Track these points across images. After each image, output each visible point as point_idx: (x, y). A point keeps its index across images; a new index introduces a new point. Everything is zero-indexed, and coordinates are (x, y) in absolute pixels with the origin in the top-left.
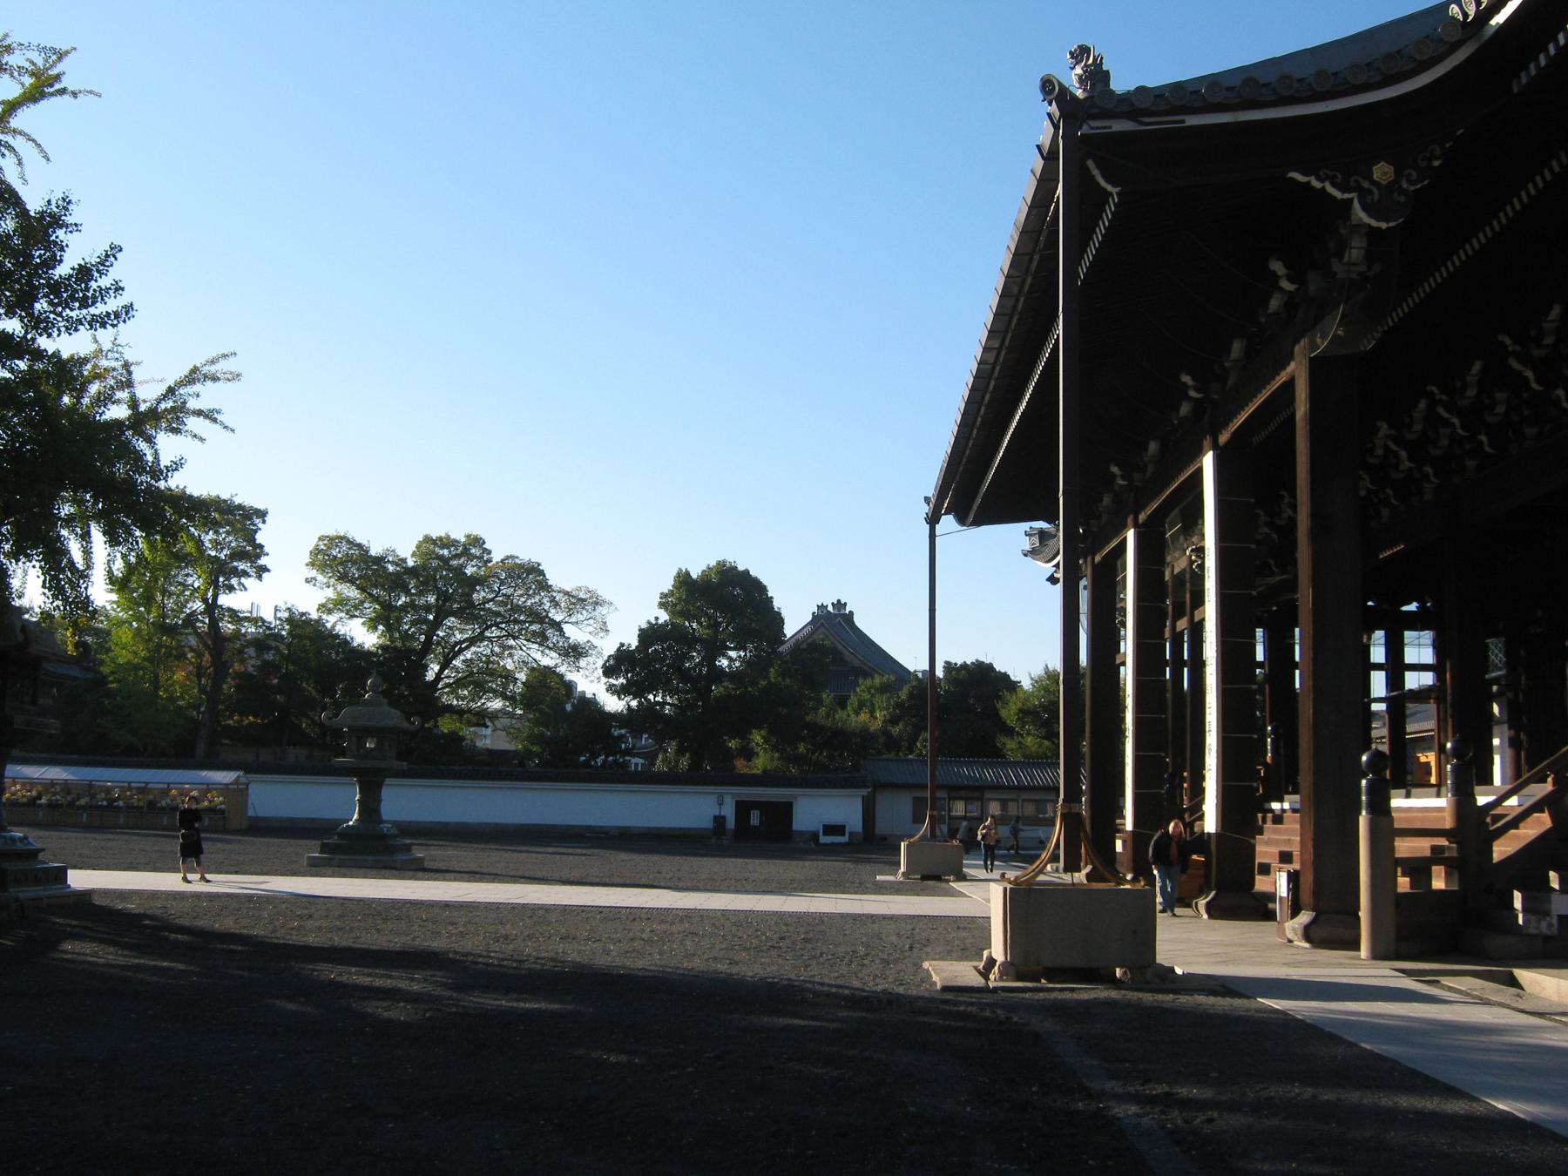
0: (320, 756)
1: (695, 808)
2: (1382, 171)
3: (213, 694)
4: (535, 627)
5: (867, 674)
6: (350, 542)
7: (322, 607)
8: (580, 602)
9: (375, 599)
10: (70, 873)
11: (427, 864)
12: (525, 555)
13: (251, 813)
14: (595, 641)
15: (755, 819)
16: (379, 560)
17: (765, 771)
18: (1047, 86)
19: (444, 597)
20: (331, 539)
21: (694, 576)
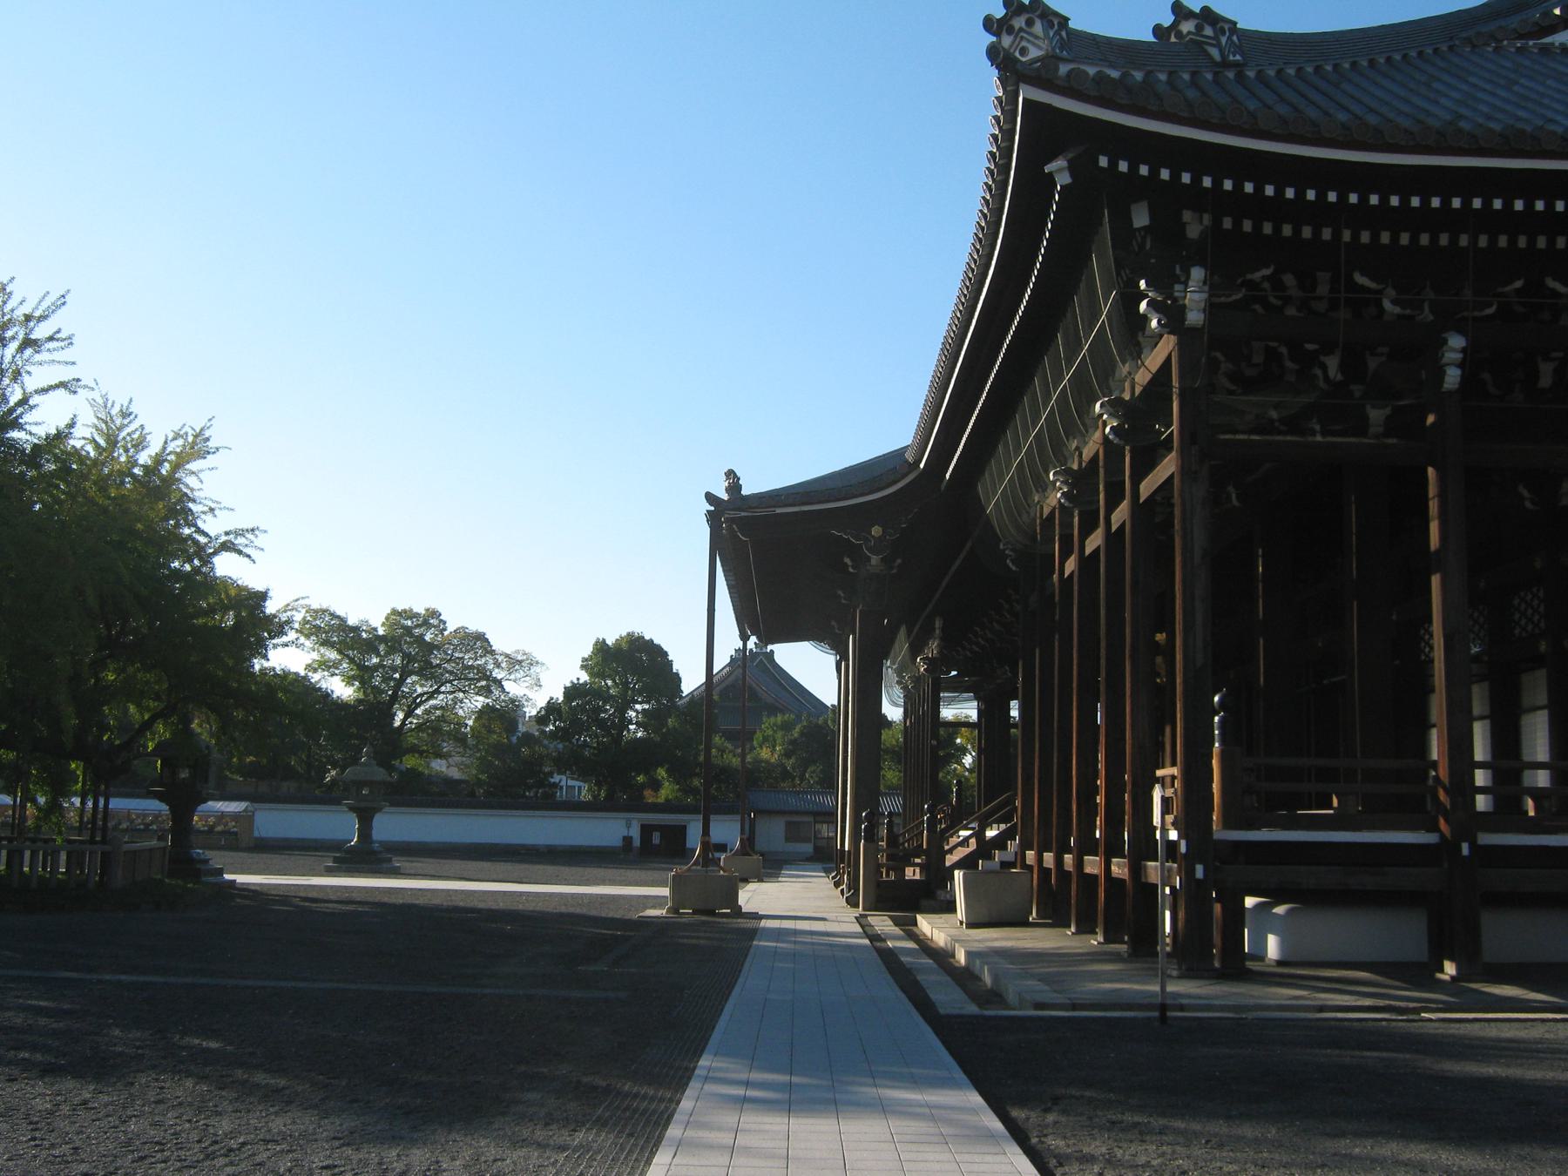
1: (609, 830)
2: (876, 531)
5: (773, 710)
6: (334, 616)
7: (309, 667)
8: (514, 663)
9: (352, 660)
12: (473, 627)
13: (256, 834)
14: (530, 694)
15: (656, 838)
16: (356, 629)
17: (667, 800)
18: (710, 497)
20: (316, 611)
21: (610, 642)
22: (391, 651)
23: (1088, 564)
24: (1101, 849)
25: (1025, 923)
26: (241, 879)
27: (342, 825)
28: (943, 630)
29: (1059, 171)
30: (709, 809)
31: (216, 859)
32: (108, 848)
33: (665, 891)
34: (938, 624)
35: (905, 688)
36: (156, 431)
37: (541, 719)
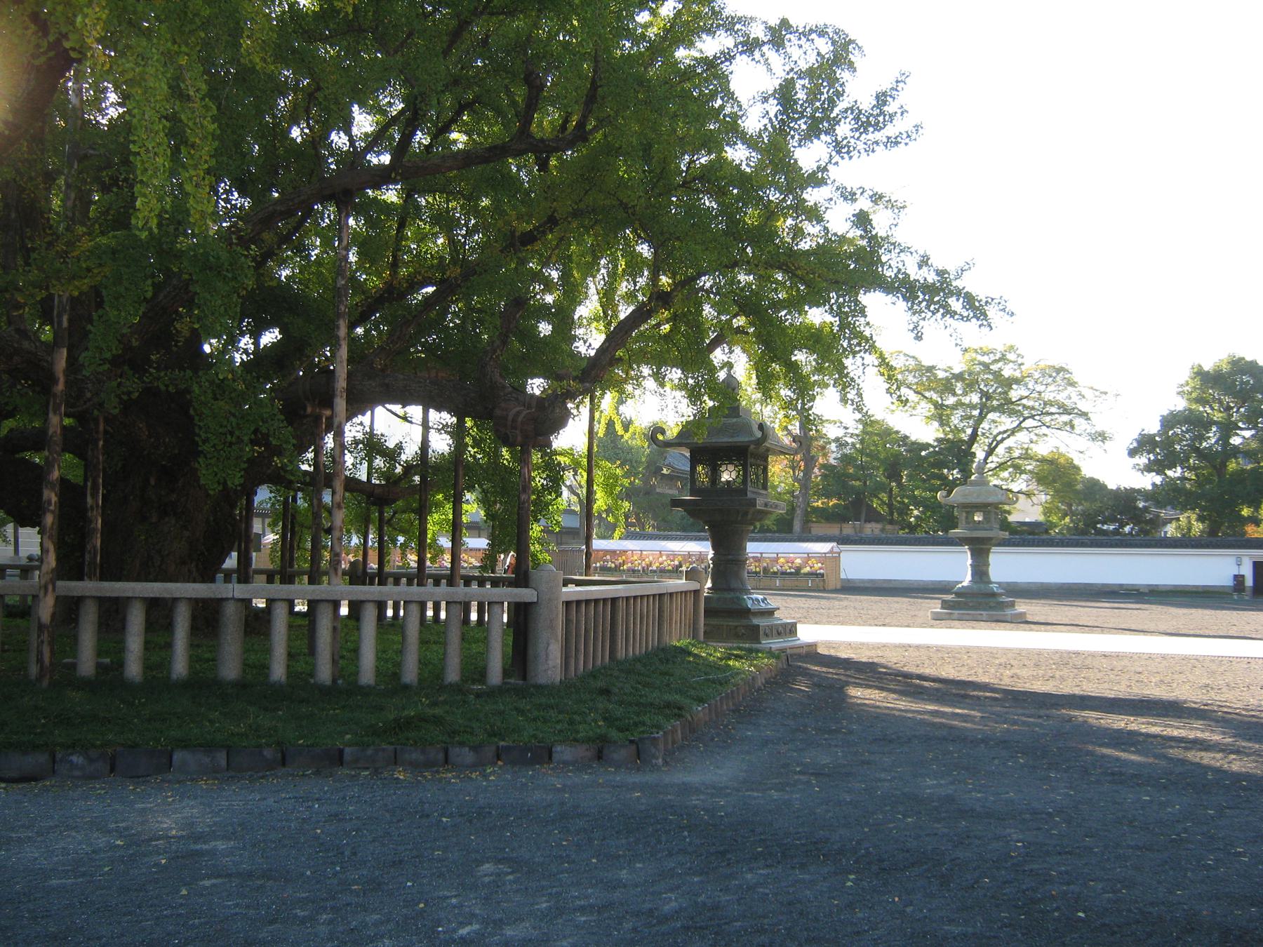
0: (939, 527)
1: (1219, 568)
3: (805, 483)
4: (1066, 418)
9: (930, 400)
10: (799, 626)
11: (1029, 618)
13: (843, 576)
16: (931, 369)
19: (987, 396)
21: (1208, 367)
31: (785, 608)
32: (526, 594)
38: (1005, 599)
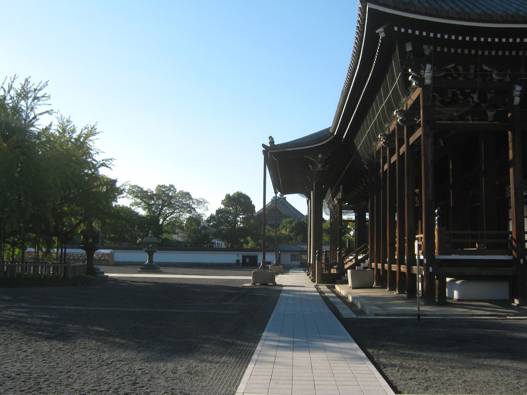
1: (232, 258)
2: (320, 156)
4: (189, 209)
5: (286, 217)
6: (139, 187)
7: (131, 205)
8: (199, 202)
9: (145, 202)
12: (185, 190)
13: (115, 260)
16: (146, 192)
17: (251, 247)
18: (264, 146)
19: (164, 201)
20: (133, 186)
21: (231, 195)
22: (158, 199)
23: (392, 166)
24: (397, 262)
25: (371, 287)
26: (110, 275)
27: (143, 257)
28: (343, 189)
29: (381, 32)
30: (265, 250)
31: (102, 268)
32: (66, 265)
33: (251, 278)
34: (341, 187)
35: (330, 209)
36: (79, 126)
37: (208, 221)
38: (157, 267)
